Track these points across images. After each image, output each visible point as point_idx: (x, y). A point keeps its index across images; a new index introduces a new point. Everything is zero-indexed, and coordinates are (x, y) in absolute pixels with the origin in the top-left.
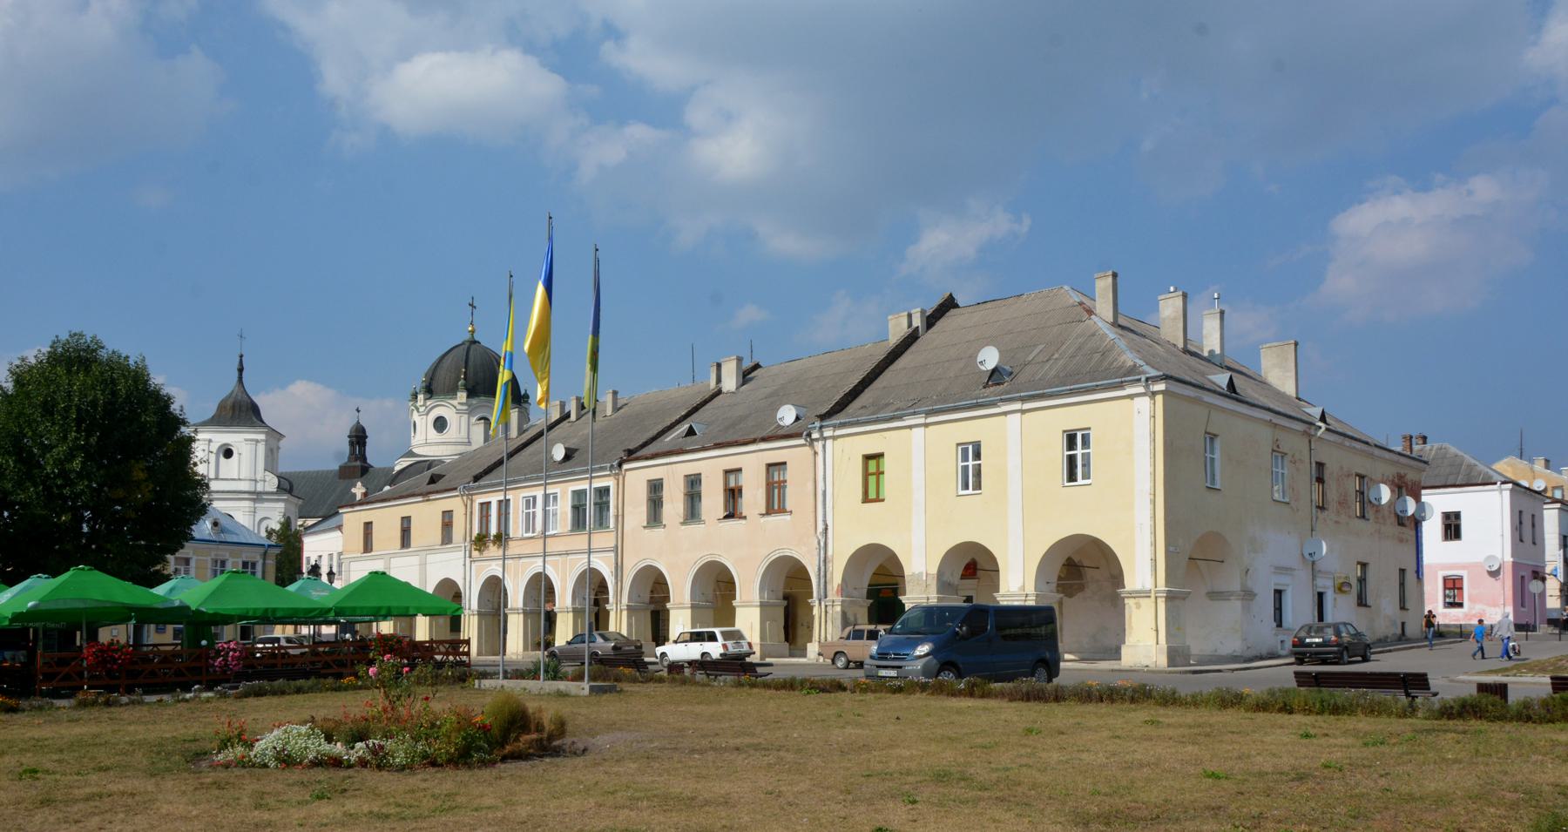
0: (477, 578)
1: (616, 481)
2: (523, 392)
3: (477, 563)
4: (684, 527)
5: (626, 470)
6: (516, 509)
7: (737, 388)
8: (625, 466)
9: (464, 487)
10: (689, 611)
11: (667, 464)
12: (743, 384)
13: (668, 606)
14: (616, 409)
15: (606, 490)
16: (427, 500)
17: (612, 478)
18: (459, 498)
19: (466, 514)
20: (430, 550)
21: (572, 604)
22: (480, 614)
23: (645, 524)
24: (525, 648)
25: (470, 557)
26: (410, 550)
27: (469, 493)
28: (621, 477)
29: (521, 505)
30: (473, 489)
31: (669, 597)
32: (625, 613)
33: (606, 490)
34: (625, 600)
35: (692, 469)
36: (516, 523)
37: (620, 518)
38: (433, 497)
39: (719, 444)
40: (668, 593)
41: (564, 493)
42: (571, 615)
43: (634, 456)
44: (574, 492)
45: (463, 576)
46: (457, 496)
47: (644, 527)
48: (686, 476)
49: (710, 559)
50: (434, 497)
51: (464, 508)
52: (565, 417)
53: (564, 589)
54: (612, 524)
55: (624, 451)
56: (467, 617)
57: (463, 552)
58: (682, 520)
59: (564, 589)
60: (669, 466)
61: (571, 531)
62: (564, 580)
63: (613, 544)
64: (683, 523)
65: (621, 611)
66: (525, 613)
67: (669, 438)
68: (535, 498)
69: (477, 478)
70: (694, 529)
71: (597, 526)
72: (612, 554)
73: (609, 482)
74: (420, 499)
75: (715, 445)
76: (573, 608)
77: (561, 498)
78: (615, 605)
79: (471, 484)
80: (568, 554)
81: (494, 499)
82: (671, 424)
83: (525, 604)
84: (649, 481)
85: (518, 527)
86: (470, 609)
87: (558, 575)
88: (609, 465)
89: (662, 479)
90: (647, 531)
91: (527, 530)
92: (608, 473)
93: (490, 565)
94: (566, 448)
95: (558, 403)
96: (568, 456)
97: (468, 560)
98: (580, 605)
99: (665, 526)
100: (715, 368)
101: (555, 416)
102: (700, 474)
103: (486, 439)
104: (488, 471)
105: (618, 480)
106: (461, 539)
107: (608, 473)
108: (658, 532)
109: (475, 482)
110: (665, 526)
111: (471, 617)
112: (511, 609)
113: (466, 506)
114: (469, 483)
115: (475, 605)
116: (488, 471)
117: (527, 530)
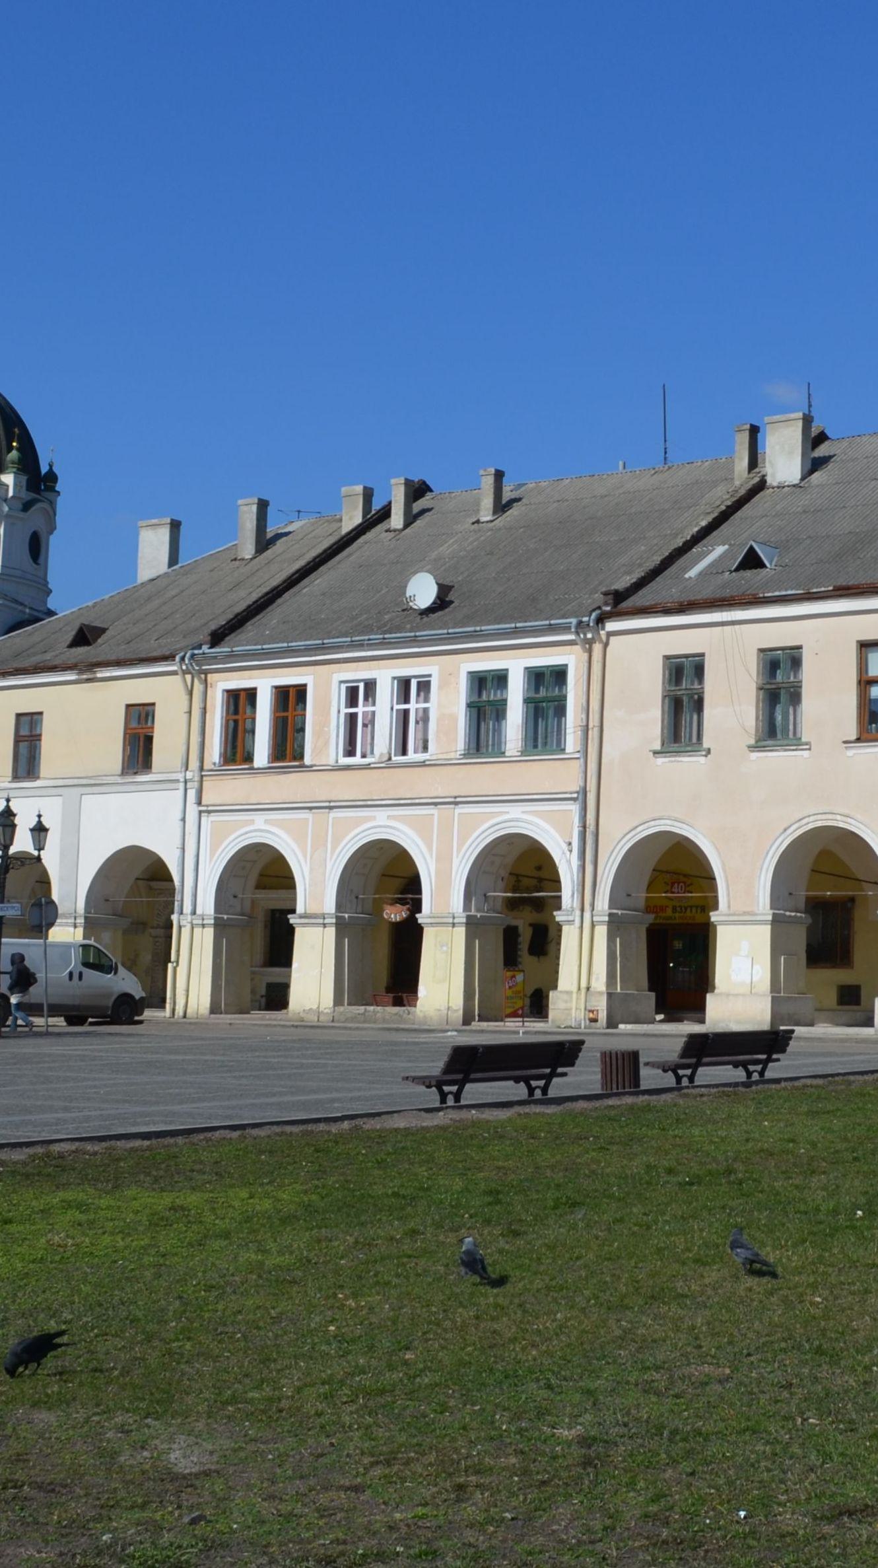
0: (213, 851)
1: (586, 655)
2: (44, 469)
3: (214, 817)
4: (755, 755)
5: (610, 634)
6: (324, 711)
7: (803, 479)
8: (611, 626)
9: (193, 656)
10: (766, 932)
11: (733, 623)
12: (812, 471)
13: (714, 917)
14: (501, 507)
15: (560, 674)
16: (88, 680)
17: (578, 648)
18: (178, 678)
19: (190, 712)
20: (94, 784)
21: (465, 910)
22: (220, 926)
23: (657, 746)
24: (338, 1001)
25: (199, 803)
26: (38, 783)
27: (200, 671)
28: (597, 648)
29: (338, 697)
30: (215, 659)
31: (716, 898)
32: (602, 932)
33: (560, 674)
34: (603, 903)
35: (779, 636)
36: (320, 733)
37: (593, 734)
38: (102, 673)
39: (848, 588)
40: (713, 887)
41: (448, 677)
42: (461, 932)
43: (625, 605)
44: (472, 675)
45: (178, 843)
46: (174, 673)
47: (655, 753)
48: (761, 650)
49: (819, 824)
50: (108, 674)
51: (186, 698)
52: (376, 518)
53: (444, 876)
54: (572, 742)
55: (606, 594)
56: (186, 932)
57: (181, 792)
58: (752, 742)
59: (444, 876)
60: (737, 627)
61: (465, 756)
62: (444, 859)
63: (575, 786)
64: (756, 747)
65: (593, 926)
66: (342, 927)
67: (696, 568)
68: (370, 686)
69: (217, 638)
70: (777, 758)
71: (530, 748)
72: (574, 808)
73: (570, 658)
74: (71, 676)
75: (837, 589)
76: (468, 917)
77: (440, 688)
78: (578, 913)
79: (205, 648)
80: (456, 803)
81: (265, 684)
82: (685, 543)
83: (339, 906)
84: (667, 658)
85: (327, 743)
86: (194, 913)
87: (430, 849)
88: (574, 621)
89: (703, 655)
90: (661, 760)
91: (350, 752)
92: (572, 637)
93: (252, 822)
94: (437, 584)
95: (359, 489)
96: (442, 603)
97: (192, 811)
98: (478, 910)
99: (709, 751)
100: (747, 434)
101: (353, 518)
102: (800, 647)
103: (173, 559)
104: (237, 623)
105: (590, 652)
106: (178, 762)
107: (572, 637)
108: (688, 764)
109: (213, 645)
110: (709, 751)
111: (197, 931)
112: (304, 916)
113: (191, 693)
114: (200, 647)
115: (207, 904)
116: (237, 623)
117: (350, 753)
